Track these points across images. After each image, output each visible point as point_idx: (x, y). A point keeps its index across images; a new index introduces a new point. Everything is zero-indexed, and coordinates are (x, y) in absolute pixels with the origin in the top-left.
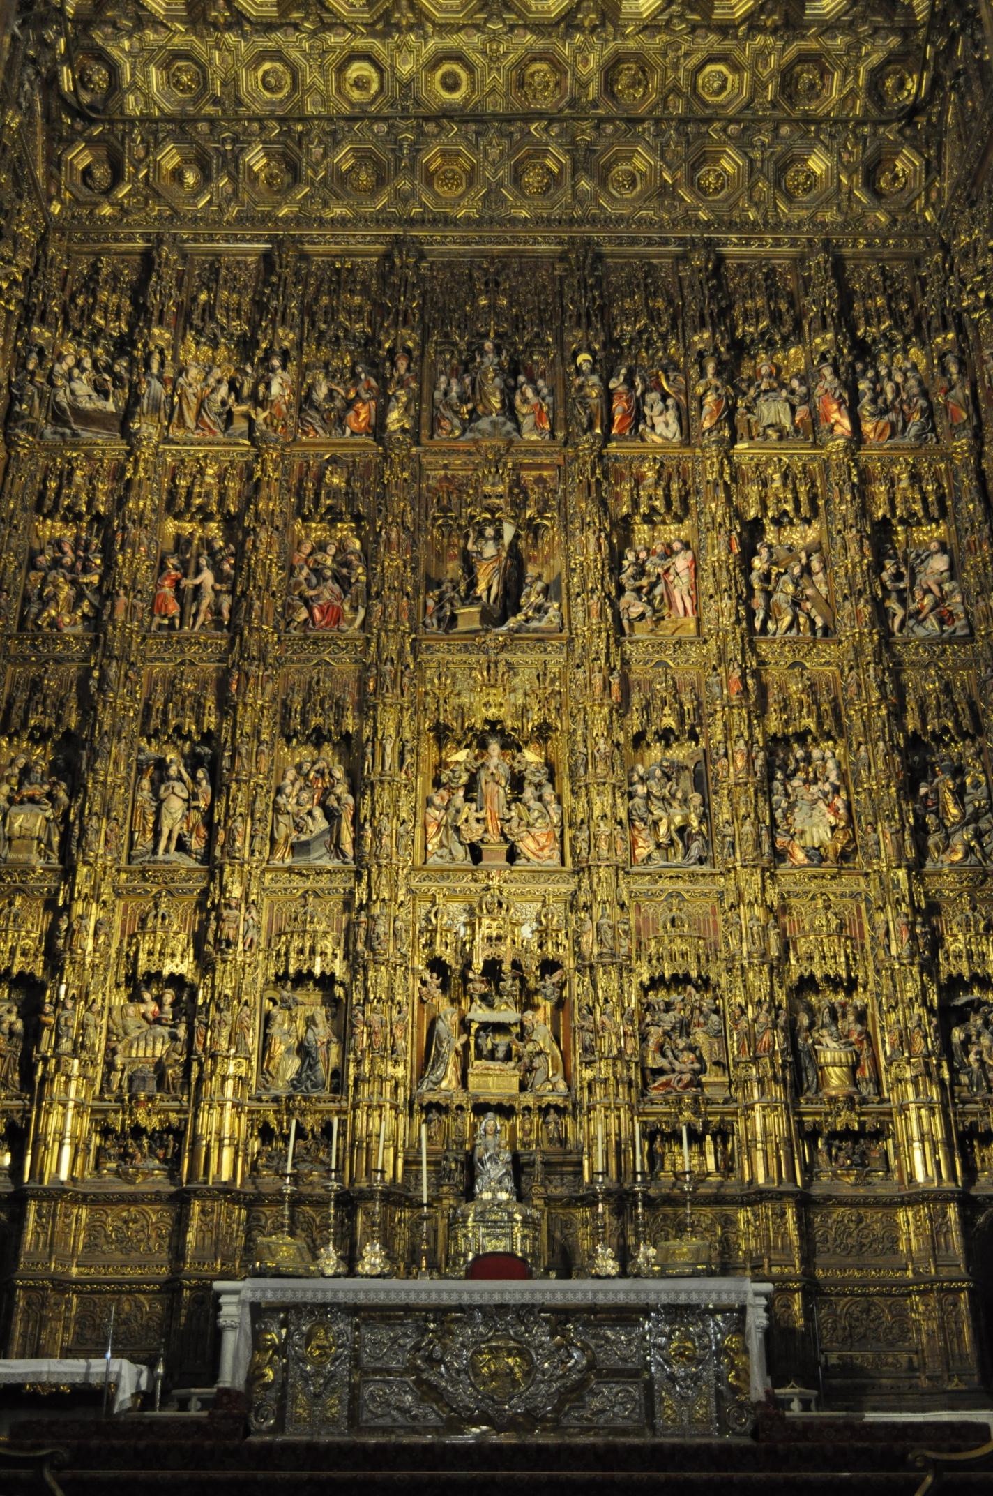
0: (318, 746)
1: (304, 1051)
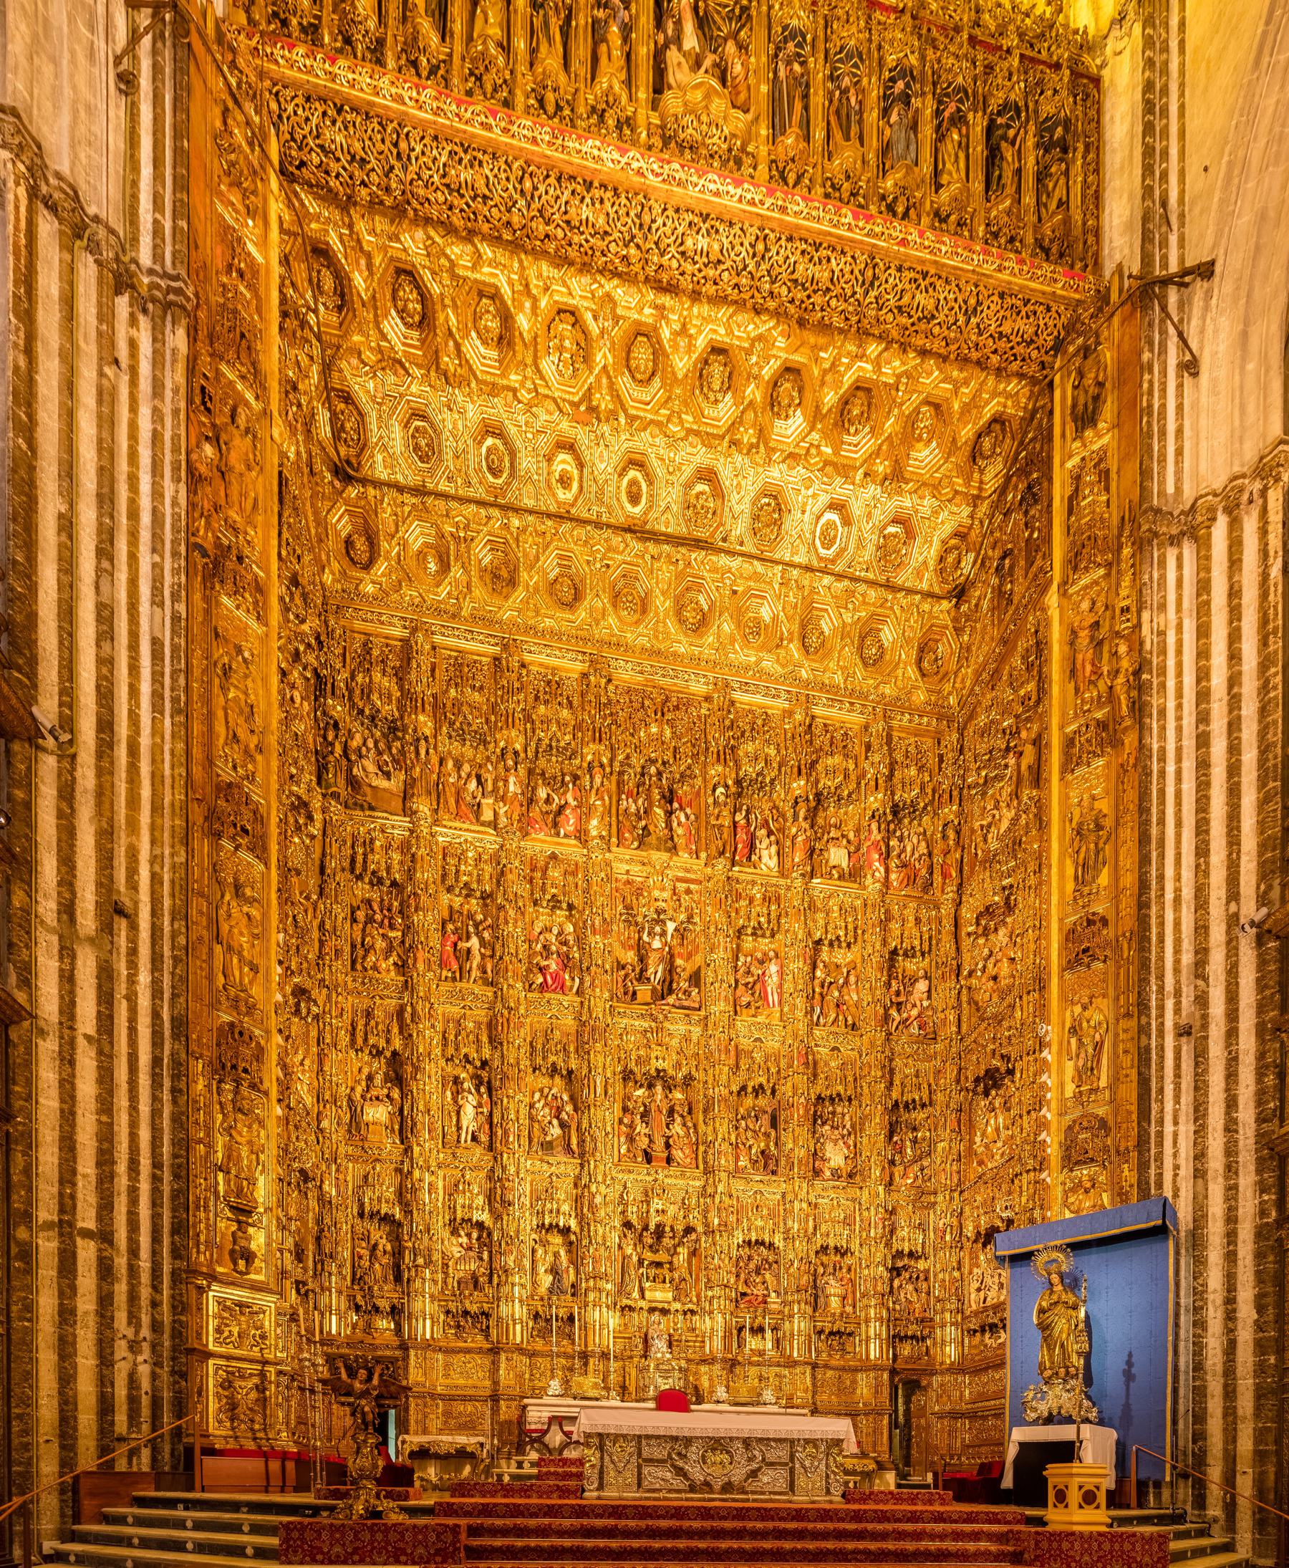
0: (552, 1077)
1: (554, 1271)
